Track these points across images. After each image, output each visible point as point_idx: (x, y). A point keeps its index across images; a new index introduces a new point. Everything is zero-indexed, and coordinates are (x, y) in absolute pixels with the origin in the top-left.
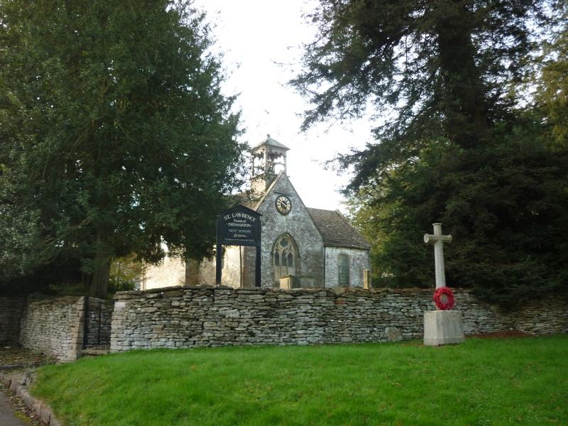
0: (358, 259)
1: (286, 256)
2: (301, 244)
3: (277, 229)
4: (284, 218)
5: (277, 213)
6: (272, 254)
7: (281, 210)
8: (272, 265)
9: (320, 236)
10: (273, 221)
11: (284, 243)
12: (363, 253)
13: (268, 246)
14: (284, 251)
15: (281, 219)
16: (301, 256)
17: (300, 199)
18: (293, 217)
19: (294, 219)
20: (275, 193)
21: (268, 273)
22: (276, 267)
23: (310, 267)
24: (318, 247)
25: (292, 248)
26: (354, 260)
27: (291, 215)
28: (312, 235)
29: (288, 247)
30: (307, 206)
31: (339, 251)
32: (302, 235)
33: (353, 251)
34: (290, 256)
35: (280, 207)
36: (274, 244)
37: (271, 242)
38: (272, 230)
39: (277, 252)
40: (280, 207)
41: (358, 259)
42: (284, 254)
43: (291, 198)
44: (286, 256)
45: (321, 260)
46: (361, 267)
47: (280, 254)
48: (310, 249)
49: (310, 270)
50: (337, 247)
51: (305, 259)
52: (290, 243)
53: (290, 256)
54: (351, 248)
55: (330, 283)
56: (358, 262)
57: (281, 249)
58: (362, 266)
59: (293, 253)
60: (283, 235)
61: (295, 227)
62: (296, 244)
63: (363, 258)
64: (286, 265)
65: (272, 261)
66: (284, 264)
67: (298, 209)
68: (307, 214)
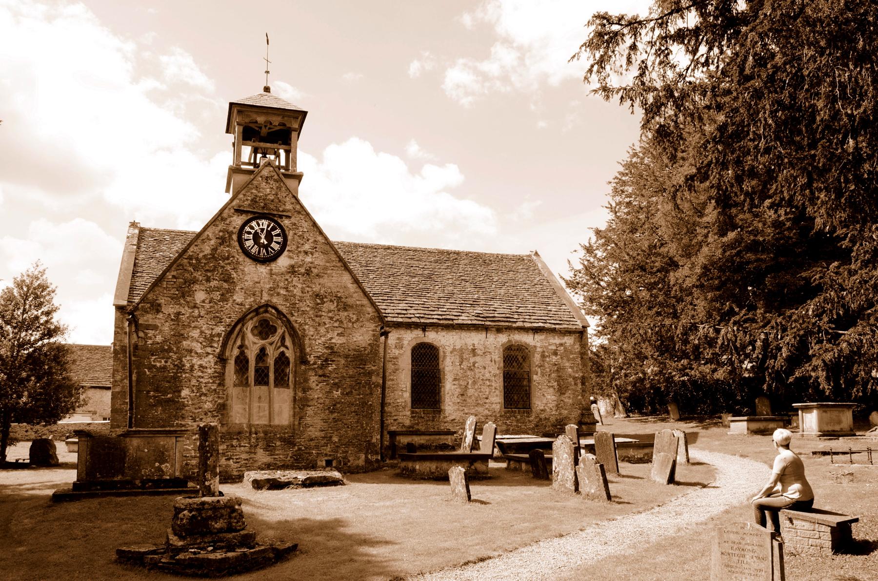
0: (555, 353)
1: (271, 361)
2: (310, 331)
3: (238, 297)
4: (263, 270)
5: (242, 258)
6: (222, 359)
7: (255, 250)
8: (221, 384)
9: (370, 309)
10: (227, 279)
11: (265, 330)
12: (569, 340)
13: (209, 340)
14: (263, 350)
15: (253, 274)
16: (311, 359)
17: (315, 224)
18: (293, 267)
19: (292, 270)
20: (239, 211)
21: (208, 406)
22: (234, 392)
23: (336, 386)
24: (362, 336)
25: (288, 342)
26: (543, 356)
27: (283, 262)
28: (346, 307)
29: (276, 338)
30: (332, 238)
31: (503, 338)
32: (317, 308)
33: (539, 337)
34: (282, 360)
35: (249, 244)
36: (229, 335)
37: (220, 329)
38: (224, 298)
39: (242, 353)
40: (249, 244)
41: (555, 353)
42: (262, 354)
43: (286, 222)
44: (271, 361)
45: (370, 367)
46: (559, 369)
47: (252, 355)
48: (338, 340)
49: (337, 393)
50: (499, 330)
51: (322, 367)
52: (280, 331)
53: (282, 360)
54: (536, 330)
55: (480, 409)
56: (554, 359)
57: (253, 344)
58: (564, 368)
59: (290, 354)
60: (257, 311)
61: (297, 292)
62: (293, 328)
63: (566, 349)
64: (267, 383)
65: (220, 377)
66: (262, 378)
67: (307, 247)
68: (333, 257)
